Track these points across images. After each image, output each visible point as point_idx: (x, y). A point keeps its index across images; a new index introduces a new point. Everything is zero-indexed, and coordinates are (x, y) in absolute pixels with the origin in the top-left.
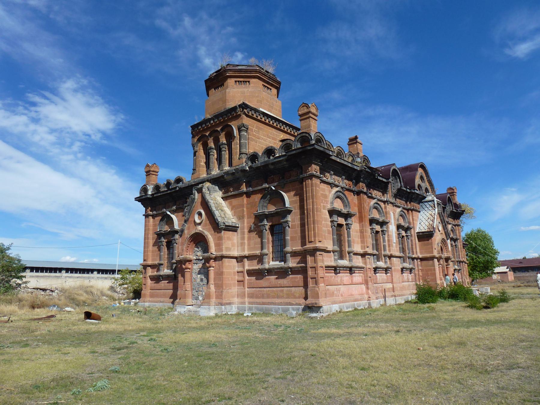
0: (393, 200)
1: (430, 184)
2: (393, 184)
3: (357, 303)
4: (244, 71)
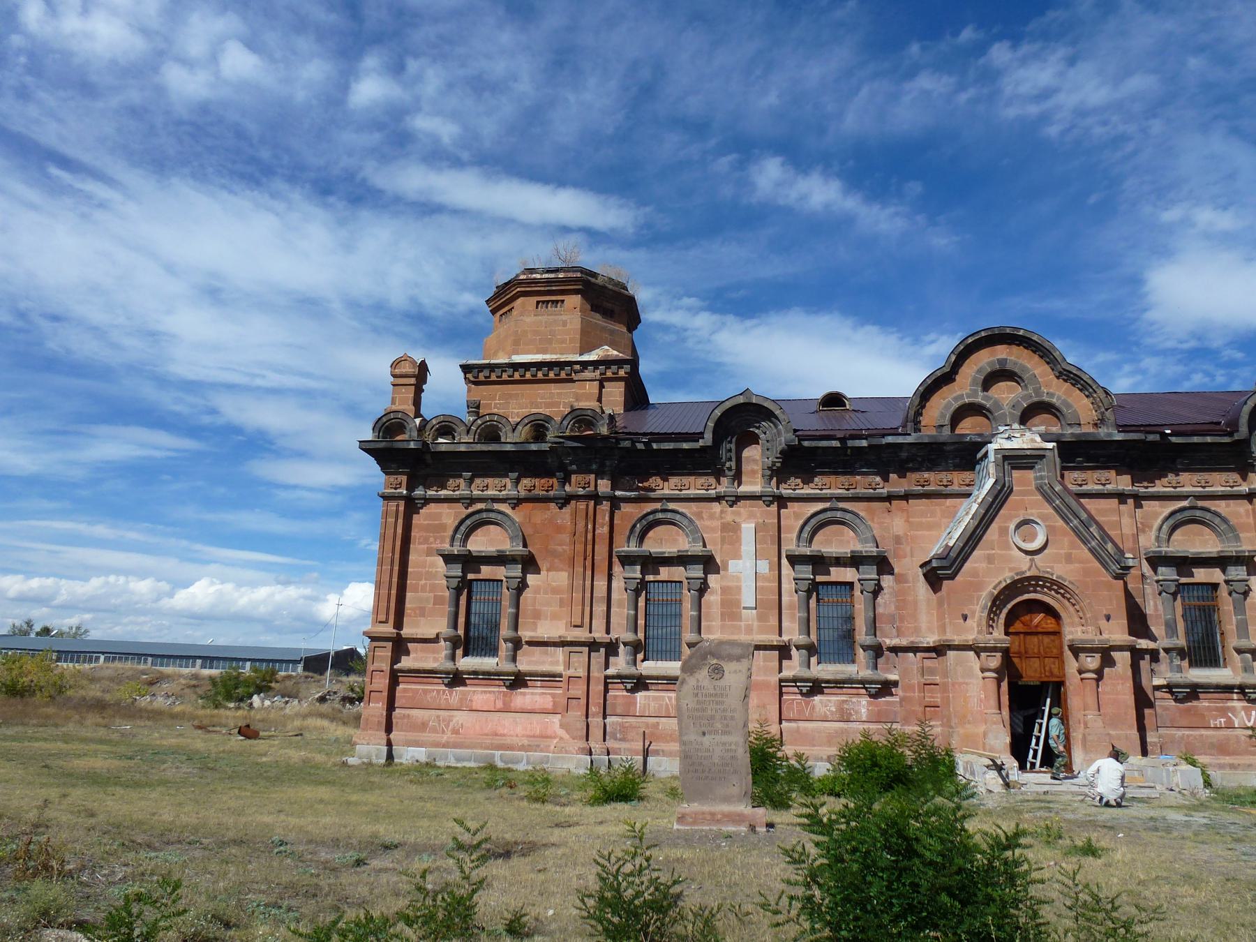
0: (772, 488)
1: (1078, 382)
2: (768, 441)
3: (501, 755)
4: (528, 283)
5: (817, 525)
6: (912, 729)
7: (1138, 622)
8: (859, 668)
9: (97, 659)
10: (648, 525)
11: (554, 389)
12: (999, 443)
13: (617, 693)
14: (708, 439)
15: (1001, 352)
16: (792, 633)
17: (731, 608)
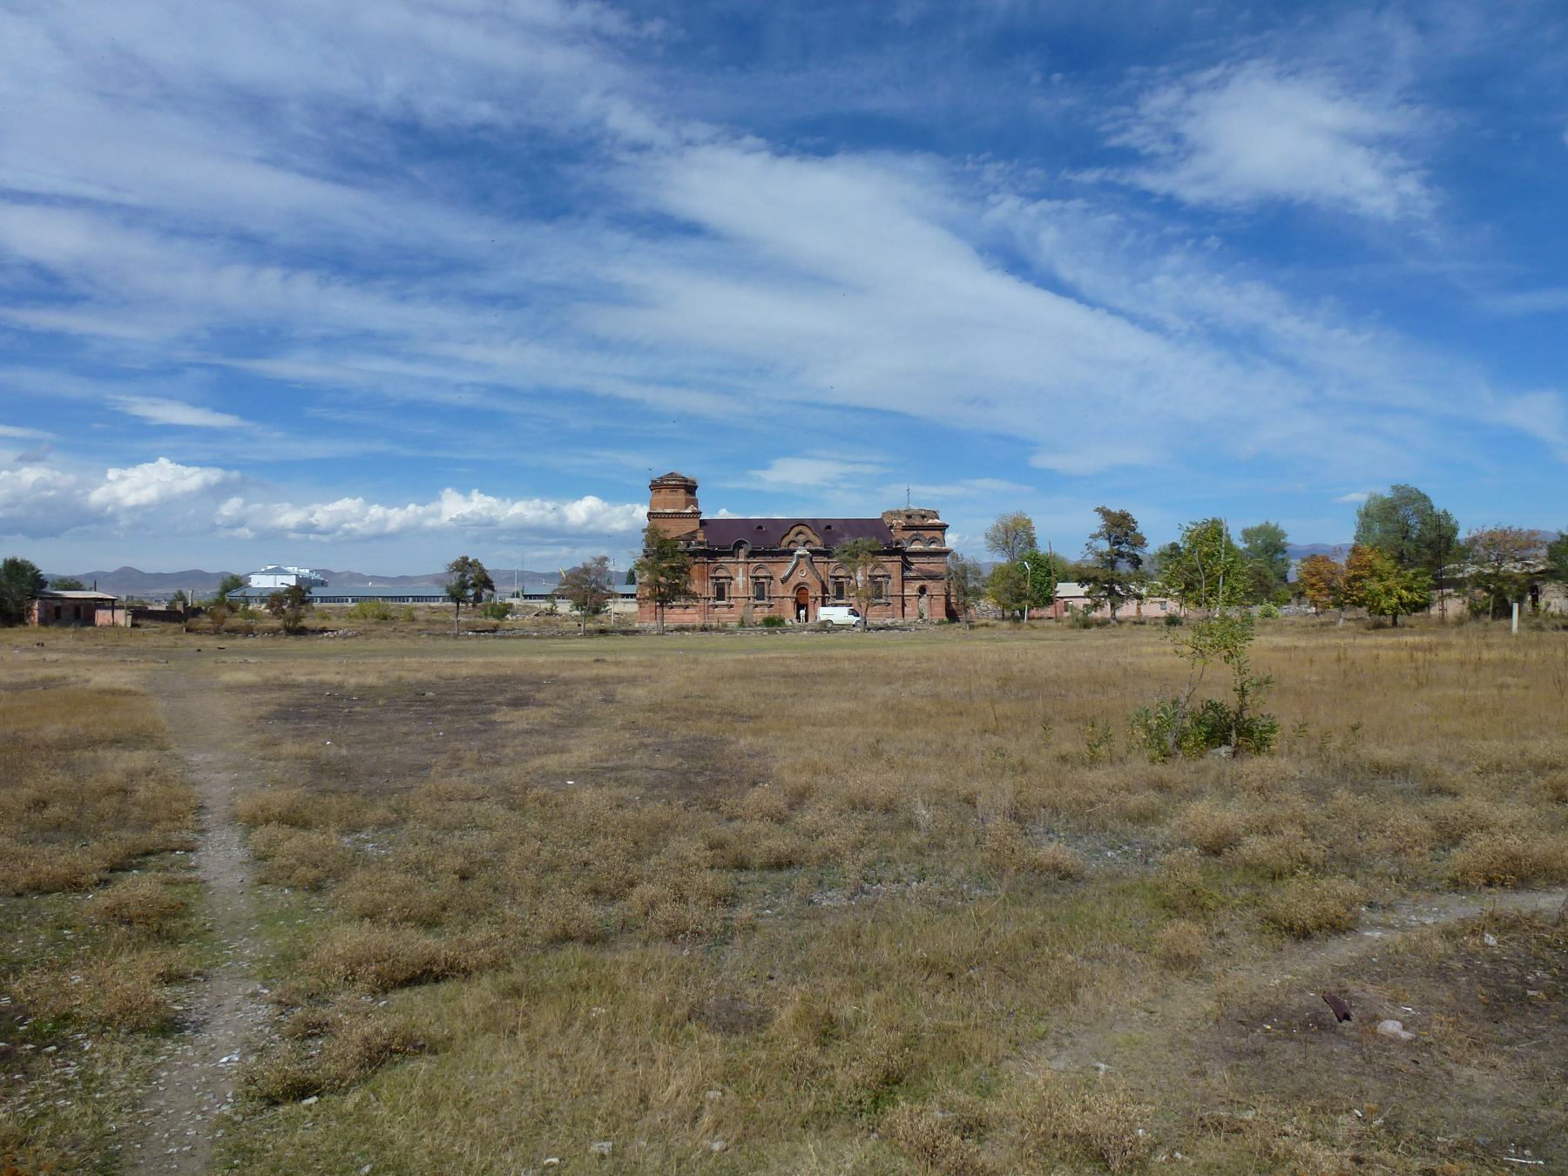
5: (757, 569)
6: (777, 614)
7: (825, 590)
8: (765, 602)
9: (347, 601)
10: (717, 569)
11: (678, 520)
12: (798, 552)
13: (711, 609)
14: (731, 549)
15: (800, 528)
16: (751, 594)
17: (737, 588)
